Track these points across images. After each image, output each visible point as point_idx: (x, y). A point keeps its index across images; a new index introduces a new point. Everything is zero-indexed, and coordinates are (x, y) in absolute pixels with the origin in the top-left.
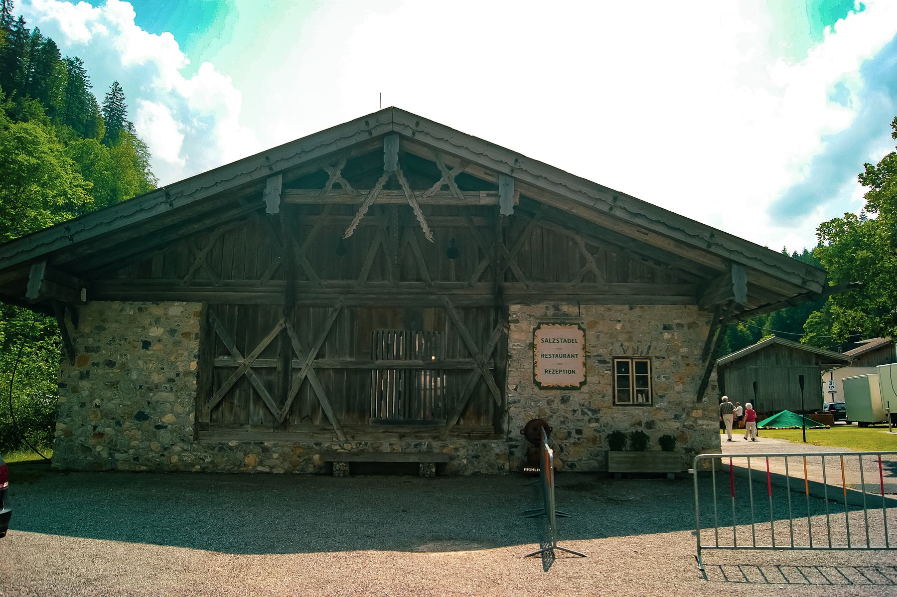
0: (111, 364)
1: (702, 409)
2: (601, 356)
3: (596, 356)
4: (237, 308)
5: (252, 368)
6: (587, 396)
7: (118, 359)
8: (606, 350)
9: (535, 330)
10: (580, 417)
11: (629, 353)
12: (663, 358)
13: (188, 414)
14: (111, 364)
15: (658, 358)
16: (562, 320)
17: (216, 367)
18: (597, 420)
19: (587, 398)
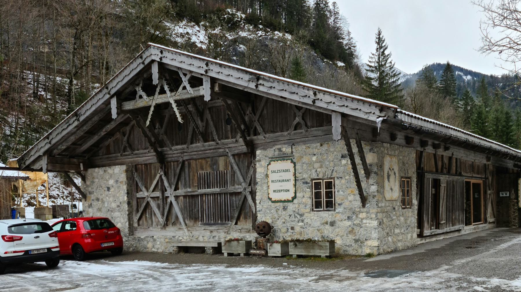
0: (98, 199)
1: (366, 212)
2: (305, 179)
3: (301, 179)
4: (143, 165)
5: (151, 198)
6: (297, 206)
7: (100, 197)
8: (307, 175)
9: (268, 165)
10: (293, 219)
11: (321, 176)
12: (341, 178)
13: (126, 223)
14: (98, 199)
15: (338, 178)
16: (283, 157)
17: (138, 198)
18: (303, 221)
19: (297, 207)
